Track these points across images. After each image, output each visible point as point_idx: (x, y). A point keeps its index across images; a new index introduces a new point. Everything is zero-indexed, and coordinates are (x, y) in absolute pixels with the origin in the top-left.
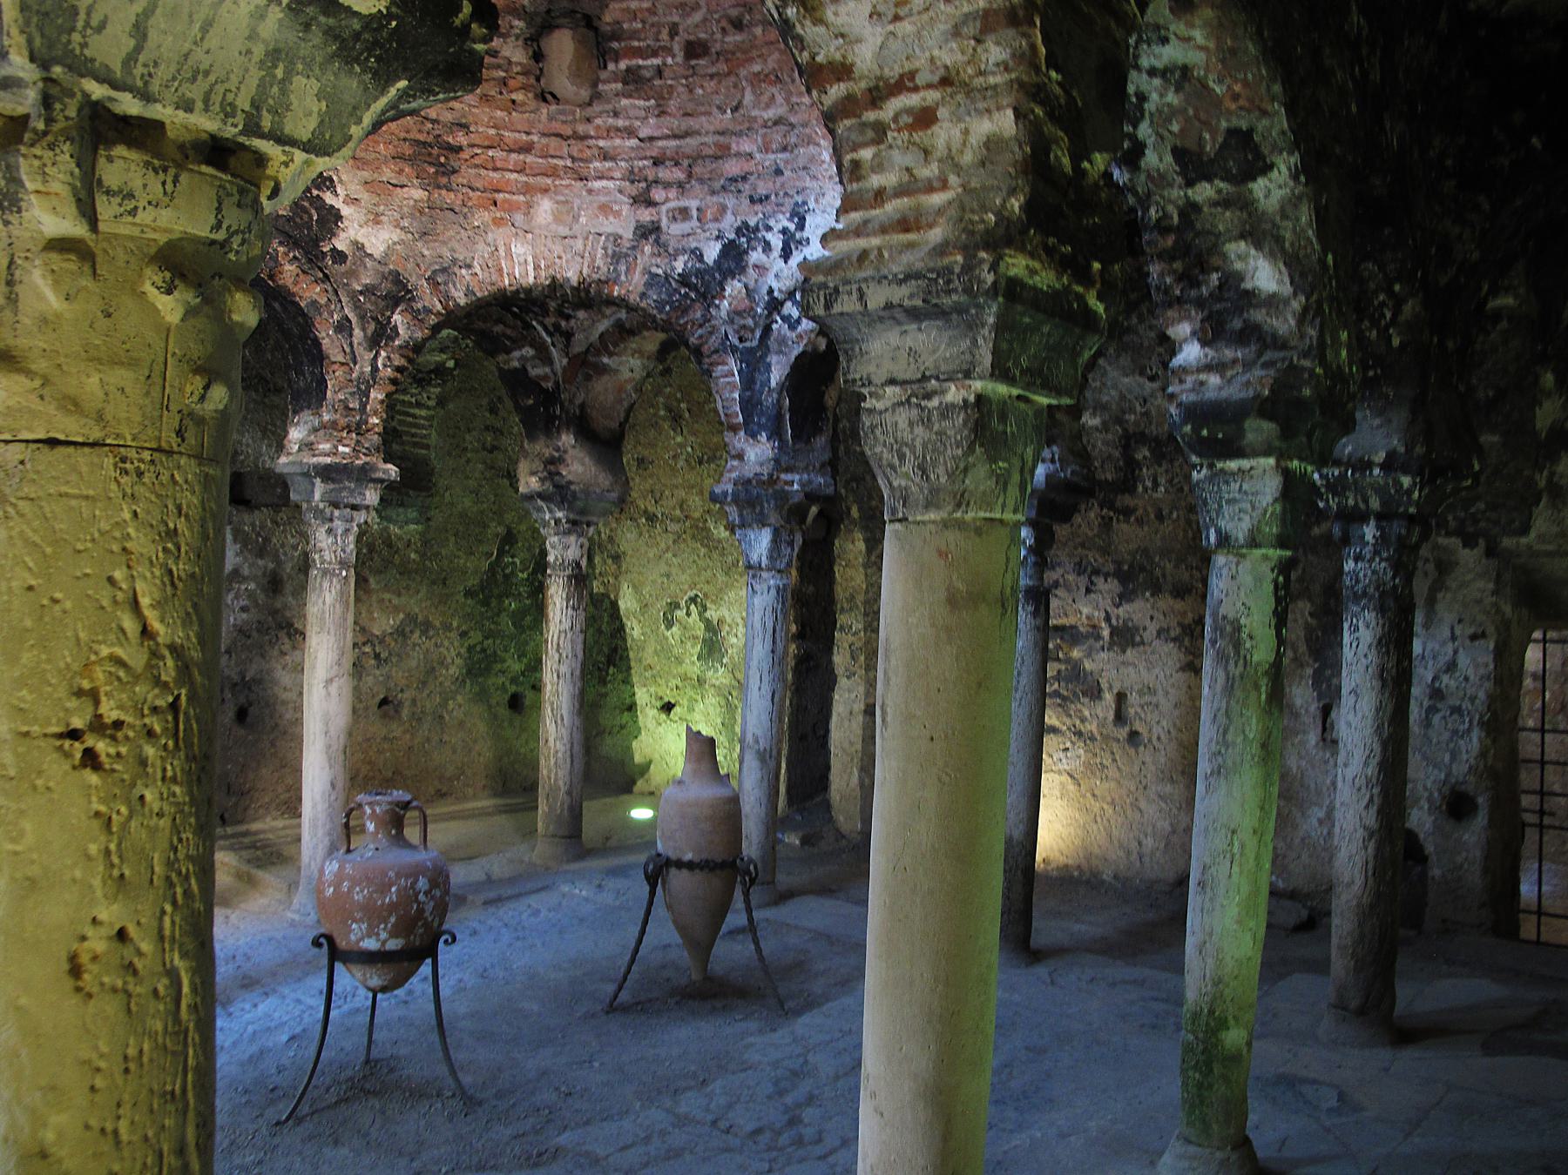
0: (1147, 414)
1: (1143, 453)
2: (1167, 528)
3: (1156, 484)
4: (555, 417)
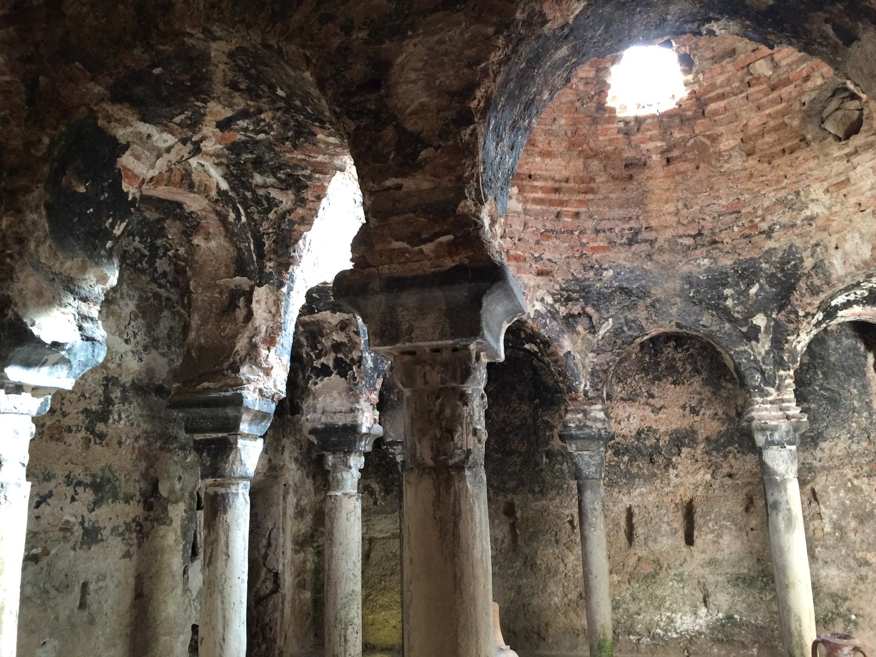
0: (119, 365)
1: (116, 394)
2: (123, 451)
3: (120, 419)
4: (108, 234)
